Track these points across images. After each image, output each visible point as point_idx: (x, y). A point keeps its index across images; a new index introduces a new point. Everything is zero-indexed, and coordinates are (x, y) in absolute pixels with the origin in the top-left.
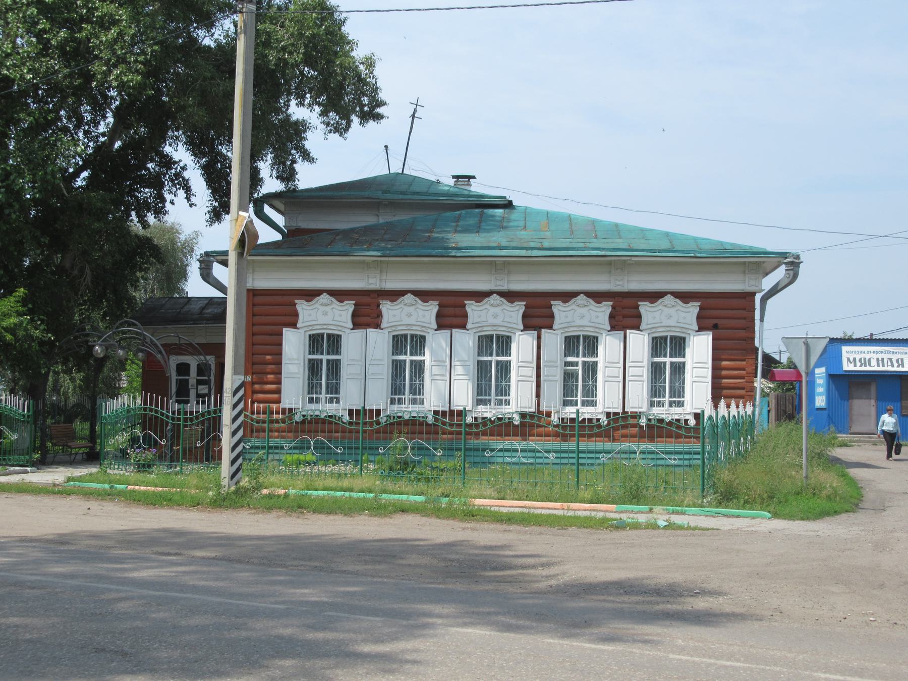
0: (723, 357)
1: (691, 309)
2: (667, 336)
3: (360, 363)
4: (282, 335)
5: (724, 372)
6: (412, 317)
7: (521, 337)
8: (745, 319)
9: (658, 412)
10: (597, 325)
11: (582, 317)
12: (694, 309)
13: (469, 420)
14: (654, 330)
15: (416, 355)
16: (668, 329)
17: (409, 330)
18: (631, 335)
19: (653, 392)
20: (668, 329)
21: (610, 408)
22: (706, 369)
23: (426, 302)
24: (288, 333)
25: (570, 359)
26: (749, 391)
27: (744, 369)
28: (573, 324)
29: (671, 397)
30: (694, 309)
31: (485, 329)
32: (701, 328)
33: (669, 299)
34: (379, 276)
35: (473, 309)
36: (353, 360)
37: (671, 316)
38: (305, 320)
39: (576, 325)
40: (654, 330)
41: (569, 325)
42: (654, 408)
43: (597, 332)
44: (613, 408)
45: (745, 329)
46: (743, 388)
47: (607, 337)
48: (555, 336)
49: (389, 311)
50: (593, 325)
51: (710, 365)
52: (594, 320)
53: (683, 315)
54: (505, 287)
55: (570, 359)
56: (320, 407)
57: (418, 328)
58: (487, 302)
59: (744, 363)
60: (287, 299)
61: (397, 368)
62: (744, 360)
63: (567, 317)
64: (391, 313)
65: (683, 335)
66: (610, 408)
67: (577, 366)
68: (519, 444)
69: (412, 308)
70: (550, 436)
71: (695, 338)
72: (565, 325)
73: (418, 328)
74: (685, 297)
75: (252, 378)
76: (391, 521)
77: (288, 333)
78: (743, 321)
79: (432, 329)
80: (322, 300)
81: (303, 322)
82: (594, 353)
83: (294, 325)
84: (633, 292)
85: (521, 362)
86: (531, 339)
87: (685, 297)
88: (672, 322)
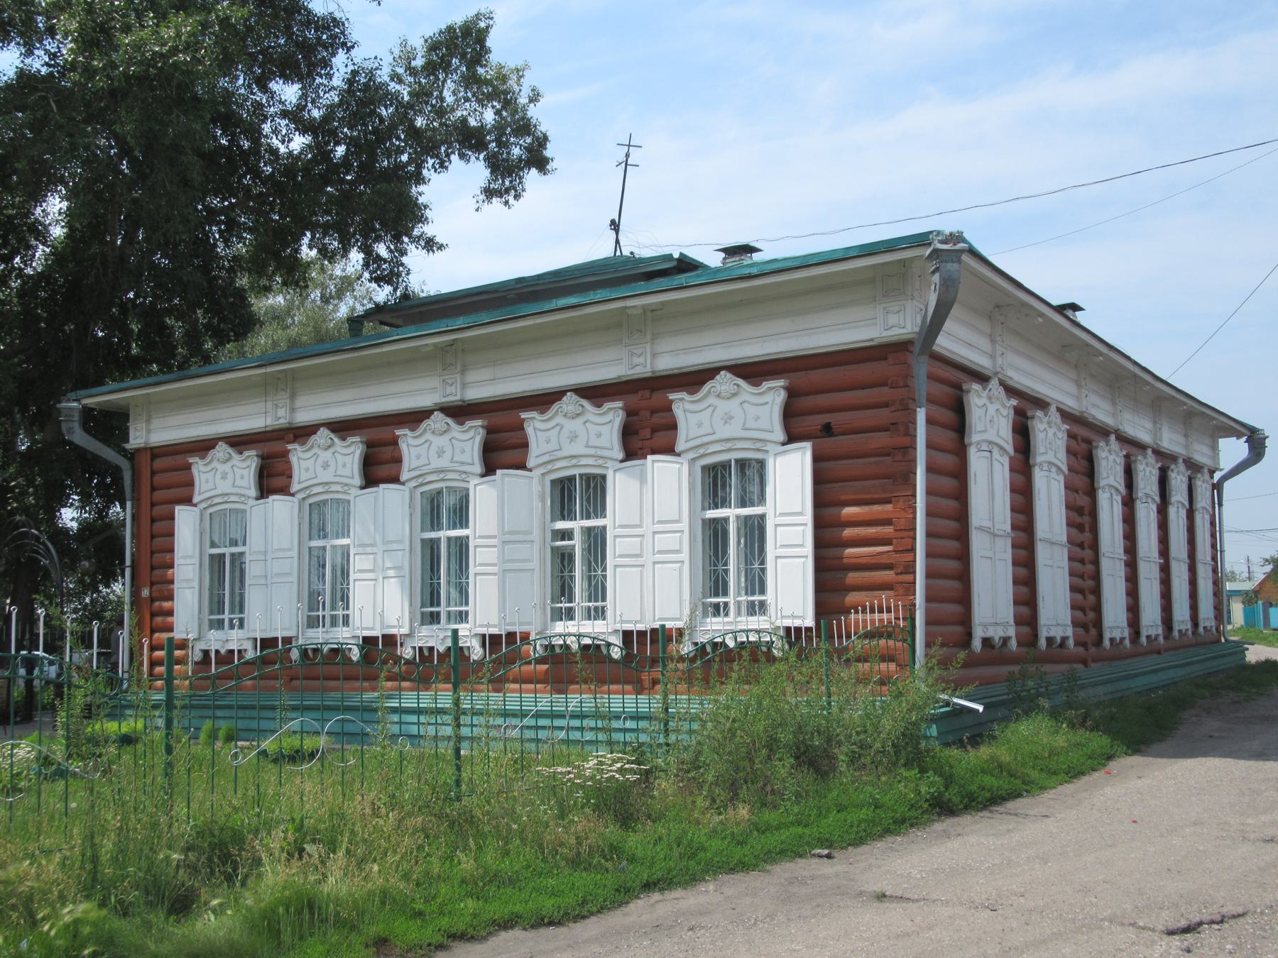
0: (843, 497)
1: (768, 398)
2: (730, 461)
3: (193, 561)
4: (173, 518)
5: (848, 532)
6: (329, 468)
7: (478, 488)
8: (886, 405)
9: (714, 628)
10: (600, 452)
11: (573, 437)
12: (773, 396)
13: (407, 653)
14: (701, 451)
15: (454, 528)
16: (729, 445)
17: (575, 466)
18: (656, 464)
19: (592, 588)
20: (729, 445)
21: (514, 624)
22: (802, 528)
23: (757, 385)
24: (181, 512)
25: (561, 525)
26: (901, 573)
27: (887, 522)
28: (559, 454)
29: (229, 614)
30: (773, 396)
31: (429, 478)
32: (792, 437)
33: (725, 382)
34: (648, 346)
35: (685, 407)
36: (280, 550)
37: (759, 418)
38: (691, 436)
39: (220, 492)
40: (701, 451)
41: (552, 458)
42: (708, 620)
43: (600, 466)
44: (363, 629)
45: (887, 430)
46: (889, 567)
47: (618, 475)
48: (527, 481)
49: (301, 461)
50: (592, 451)
51: (808, 518)
52: (594, 441)
53: (752, 411)
54: (454, 395)
55: (561, 525)
56: (571, 627)
57: (590, 461)
58: (425, 430)
59: (889, 507)
60: (178, 459)
61: (715, 534)
62: (888, 501)
63: (548, 441)
64: (693, 419)
65: (759, 456)
66: (514, 624)
67: (571, 538)
68: (620, 701)
69: (328, 454)
70: (339, 679)
71: (780, 460)
72: (546, 458)
73: (590, 461)
74: (753, 372)
75: (151, 593)
76: (827, 868)
77: (181, 512)
78: (884, 412)
79: (355, 486)
80: (718, 386)
81: (299, 483)
82: (600, 510)
83: (188, 501)
84: (352, 420)
85: (620, 526)
86: (637, 484)
87: (753, 372)
88: (733, 430)
